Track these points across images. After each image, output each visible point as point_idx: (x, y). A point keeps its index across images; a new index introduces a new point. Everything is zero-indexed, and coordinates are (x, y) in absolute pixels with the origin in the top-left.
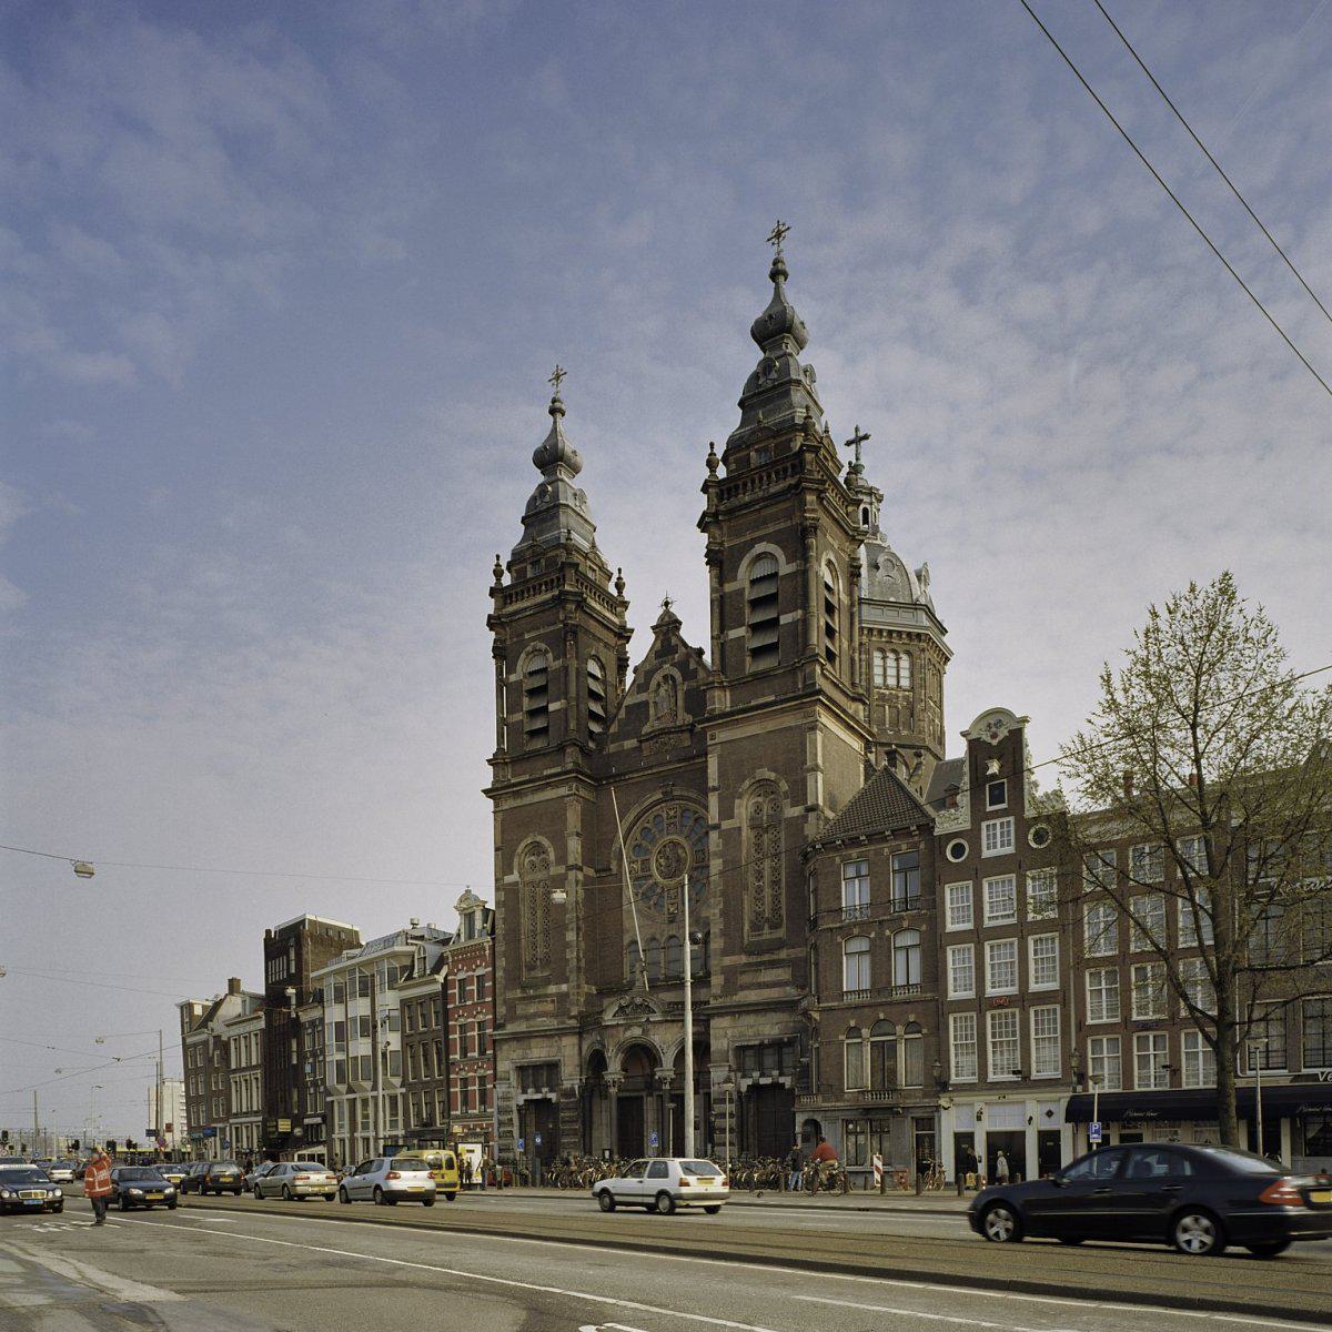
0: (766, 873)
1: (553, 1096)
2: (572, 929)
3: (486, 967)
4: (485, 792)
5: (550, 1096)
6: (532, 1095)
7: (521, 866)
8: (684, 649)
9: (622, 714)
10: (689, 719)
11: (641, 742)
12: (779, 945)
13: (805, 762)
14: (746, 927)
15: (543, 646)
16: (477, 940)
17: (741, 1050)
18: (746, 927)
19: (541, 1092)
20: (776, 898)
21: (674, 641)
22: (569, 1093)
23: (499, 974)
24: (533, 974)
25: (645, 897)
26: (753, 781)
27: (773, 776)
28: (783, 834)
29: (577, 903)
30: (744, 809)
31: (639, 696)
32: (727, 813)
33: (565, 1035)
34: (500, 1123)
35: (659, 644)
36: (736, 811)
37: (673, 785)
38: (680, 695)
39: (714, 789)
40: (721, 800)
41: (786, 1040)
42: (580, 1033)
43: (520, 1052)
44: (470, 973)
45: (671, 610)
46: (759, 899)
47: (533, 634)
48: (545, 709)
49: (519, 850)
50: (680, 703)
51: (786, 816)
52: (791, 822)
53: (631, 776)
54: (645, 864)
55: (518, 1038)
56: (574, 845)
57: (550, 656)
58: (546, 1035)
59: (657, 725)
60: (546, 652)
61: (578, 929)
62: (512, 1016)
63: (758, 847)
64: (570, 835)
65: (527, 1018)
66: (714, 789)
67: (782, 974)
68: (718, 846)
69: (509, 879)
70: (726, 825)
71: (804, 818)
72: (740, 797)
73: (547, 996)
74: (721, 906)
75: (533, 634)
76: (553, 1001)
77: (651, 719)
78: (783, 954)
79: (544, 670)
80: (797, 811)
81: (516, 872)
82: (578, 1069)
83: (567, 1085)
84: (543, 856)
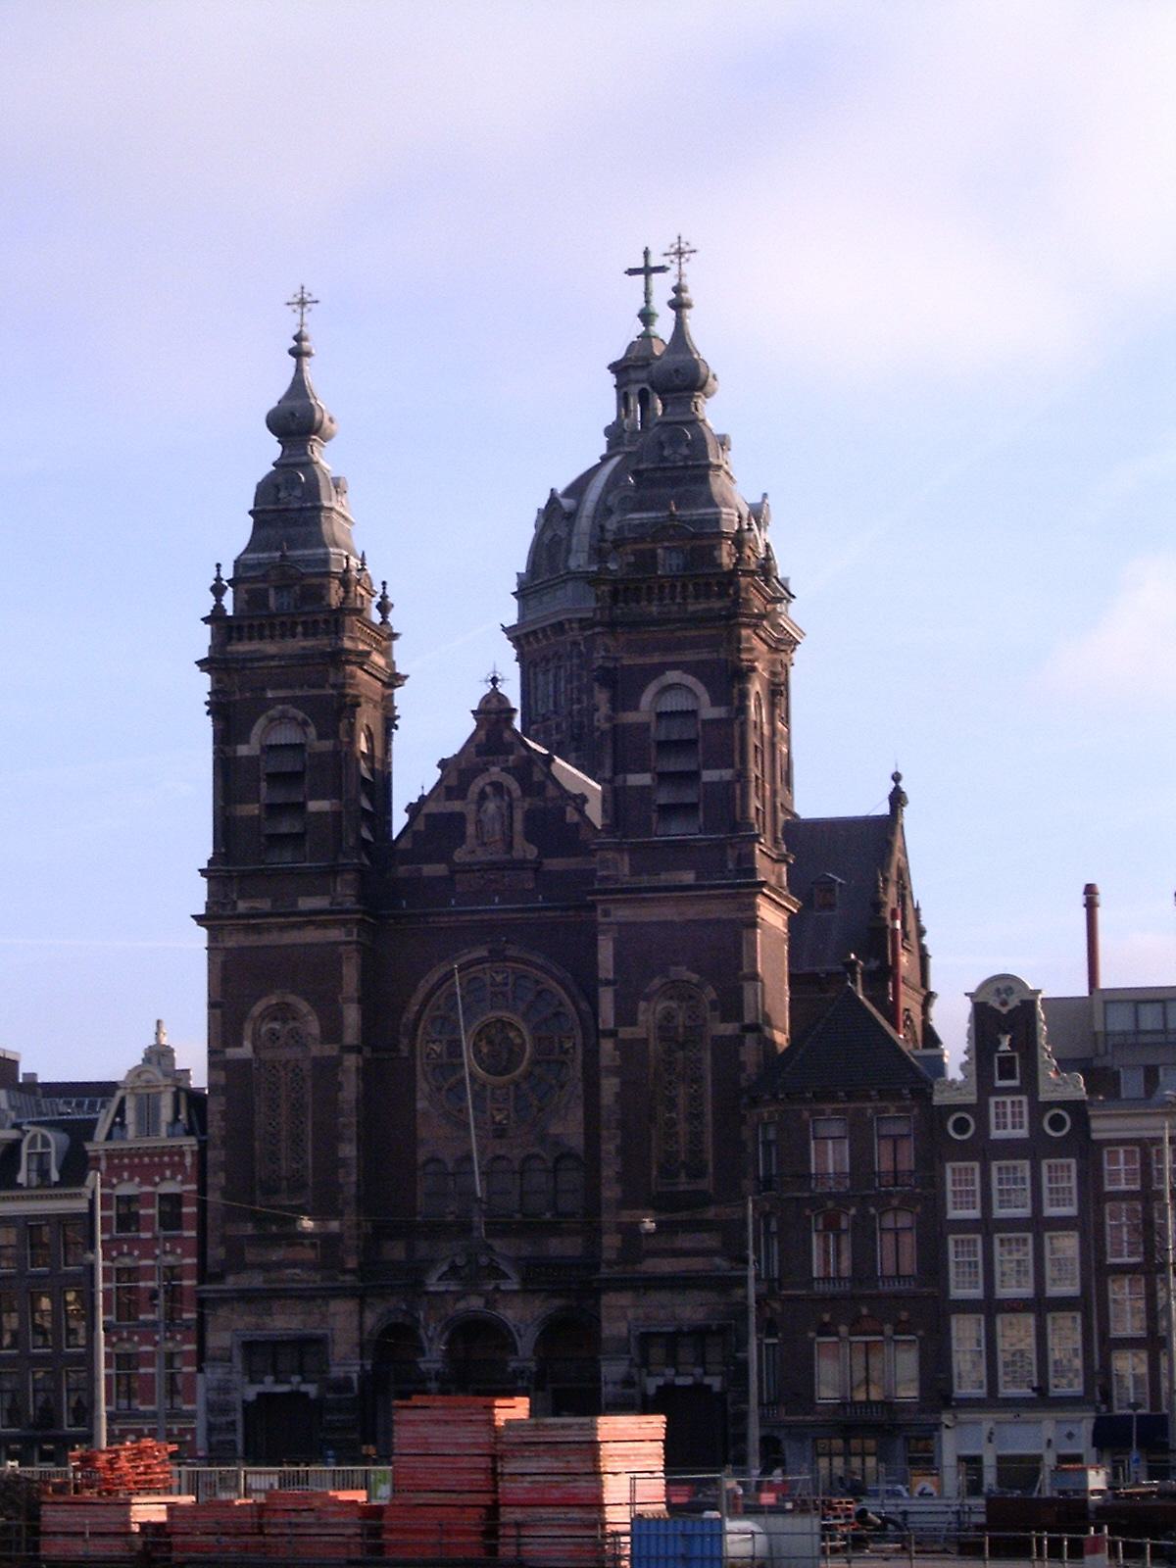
0: (681, 1101)
1: (311, 1389)
2: (350, 1141)
3: (183, 1182)
4: (198, 918)
5: (304, 1388)
6: (269, 1385)
7: (256, 1035)
8: (524, 752)
9: (420, 825)
10: (532, 852)
11: (453, 872)
14: (654, 1173)
15: (301, 715)
16: (162, 1139)
17: (646, 1339)
18: (654, 1173)
19: (289, 1383)
22: (343, 1385)
23: (214, 1198)
26: (664, 980)
27: (695, 978)
29: (357, 1100)
30: (649, 1015)
31: (447, 803)
32: (626, 1016)
33: (335, 1297)
34: (211, 1428)
35: (482, 733)
36: (641, 1018)
37: (506, 942)
38: (518, 816)
39: (608, 983)
40: (618, 997)
41: (714, 1328)
42: (361, 1296)
43: (251, 1320)
44: (148, 1189)
45: (500, 691)
47: (281, 693)
48: (302, 806)
49: (257, 1009)
50: (518, 826)
51: (714, 1033)
52: (719, 1042)
53: (437, 919)
54: (454, 1049)
55: (247, 1297)
56: (352, 1015)
57: (312, 731)
58: (306, 1296)
59: (482, 856)
60: (304, 724)
61: (359, 1138)
62: (236, 1263)
64: (348, 1000)
65: (266, 1267)
66: (608, 983)
67: (710, 1240)
68: (614, 1060)
69: (233, 1053)
70: (625, 1033)
71: (739, 1040)
72: (648, 998)
74: (618, 1141)
75: (281, 693)
76: (313, 1246)
77: (468, 840)
78: (710, 1213)
79: (298, 747)
80: (728, 1029)
81: (248, 1045)
82: (357, 1350)
83: (337, 1372)
84: (292, 1024)
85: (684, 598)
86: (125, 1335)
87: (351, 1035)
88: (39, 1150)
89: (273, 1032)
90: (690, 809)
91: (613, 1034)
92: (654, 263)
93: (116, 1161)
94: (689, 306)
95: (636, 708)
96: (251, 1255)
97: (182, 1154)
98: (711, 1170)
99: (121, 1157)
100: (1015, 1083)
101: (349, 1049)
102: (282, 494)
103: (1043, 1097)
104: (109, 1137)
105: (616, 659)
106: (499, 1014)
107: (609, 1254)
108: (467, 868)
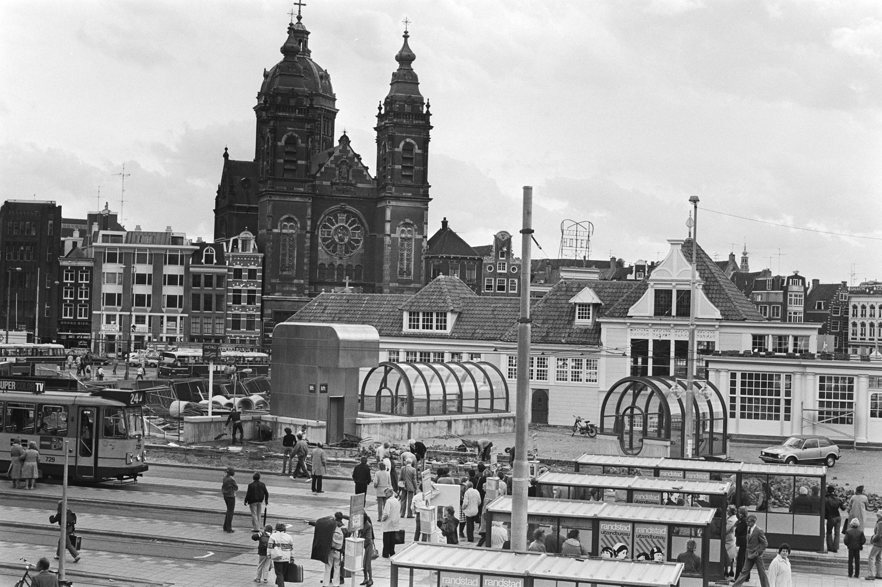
3: (257, 266)
8: (352, 153)
12: (410, 282)
13: (423, 220)
20: (408, 265)
21: (348, 149)
23: (268, 271)
24: (284, 273)
25: (328, 246)
27: (412, 222)
28: (413, 243)
32: (393, 231)
35: (341, 148)
45: (347, 134)
46: (402, 264)
49: (282, 219)
56: (309, 223)
63: (402, 245)
64: (309, 219)
69: (275, 231)
72: (399, 227)
80: (420, 237)
85: (412, 119)
87: (308, 228)
90: (410, 177)
91: (389, 235)
92: (302, 2)
94: (408, 36)
95: (398, 147)
96: (277, 288)
98: (412, 274)
100: (504, 259)
102: (290, 70)
103: (511, 263)
104: (232, 251)
105: (394, 133)
106: (342, 224)
108: (338, 184)
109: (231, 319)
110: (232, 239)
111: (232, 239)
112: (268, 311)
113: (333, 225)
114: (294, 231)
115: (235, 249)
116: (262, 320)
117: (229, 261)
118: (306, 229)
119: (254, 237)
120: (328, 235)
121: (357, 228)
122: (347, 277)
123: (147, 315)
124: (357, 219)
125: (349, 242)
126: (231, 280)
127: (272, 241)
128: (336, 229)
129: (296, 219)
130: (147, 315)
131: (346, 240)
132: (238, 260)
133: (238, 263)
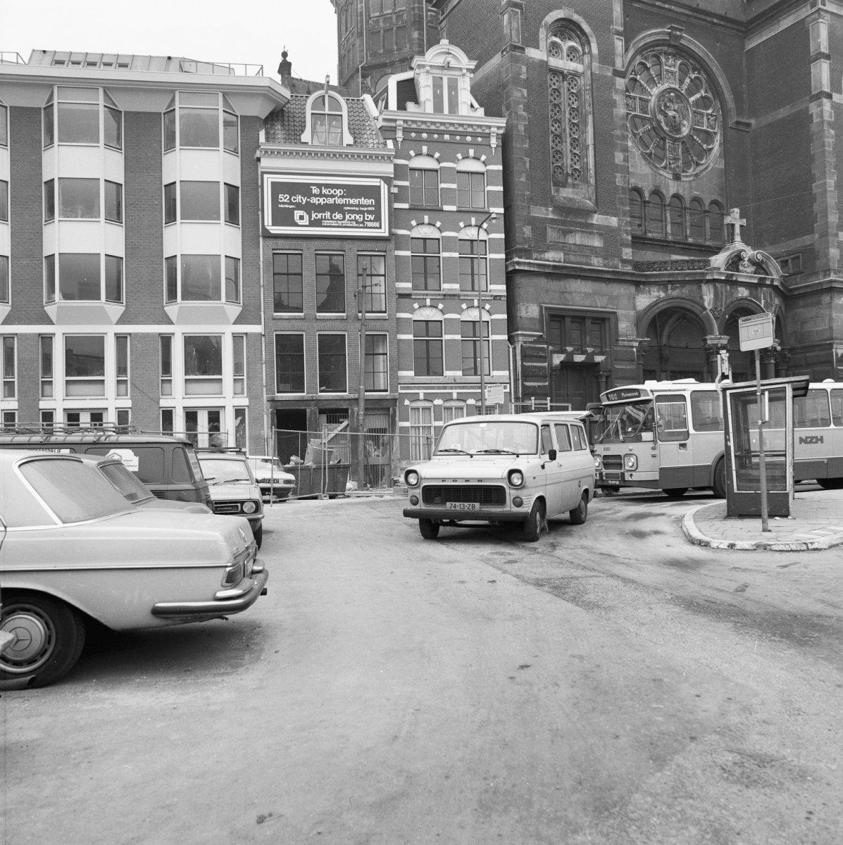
23: (520, 179)
40: (832, 71)
62: (541, 244)
66: (827, 57)
69: (532, 53)
73: (592, 224)
76: (600, 235)
86: (428, 302)
88: (327, 111)
89: (554, 44)
91: (829, 96)
93: (413, 135)
96: (552, 235)
97: (488, 136)
99: (419, 132)
101: (617, 73)
107: (834, 265)
109: (411, 337)
110: (392, 82)
111: (392, 82)
112: (529, 311)
113: (651, 81)
114: (579, 68)
115: (410, 106)
116: (511, 340)
117: (395, 140)
118: (613, 64)
119: (472, 65)
120: (644, 110)
121: (704, 103)
122: (737, 210)
123: (110, 332)
124: (703, 77)
125: (690, 136)
126: (406, 206)
127: (527, 84)
128: (662, 95)
129: (586, 27)
130: (110, 332)
131: (685, 131)
132: (426, 141)
133: (425, 149)
